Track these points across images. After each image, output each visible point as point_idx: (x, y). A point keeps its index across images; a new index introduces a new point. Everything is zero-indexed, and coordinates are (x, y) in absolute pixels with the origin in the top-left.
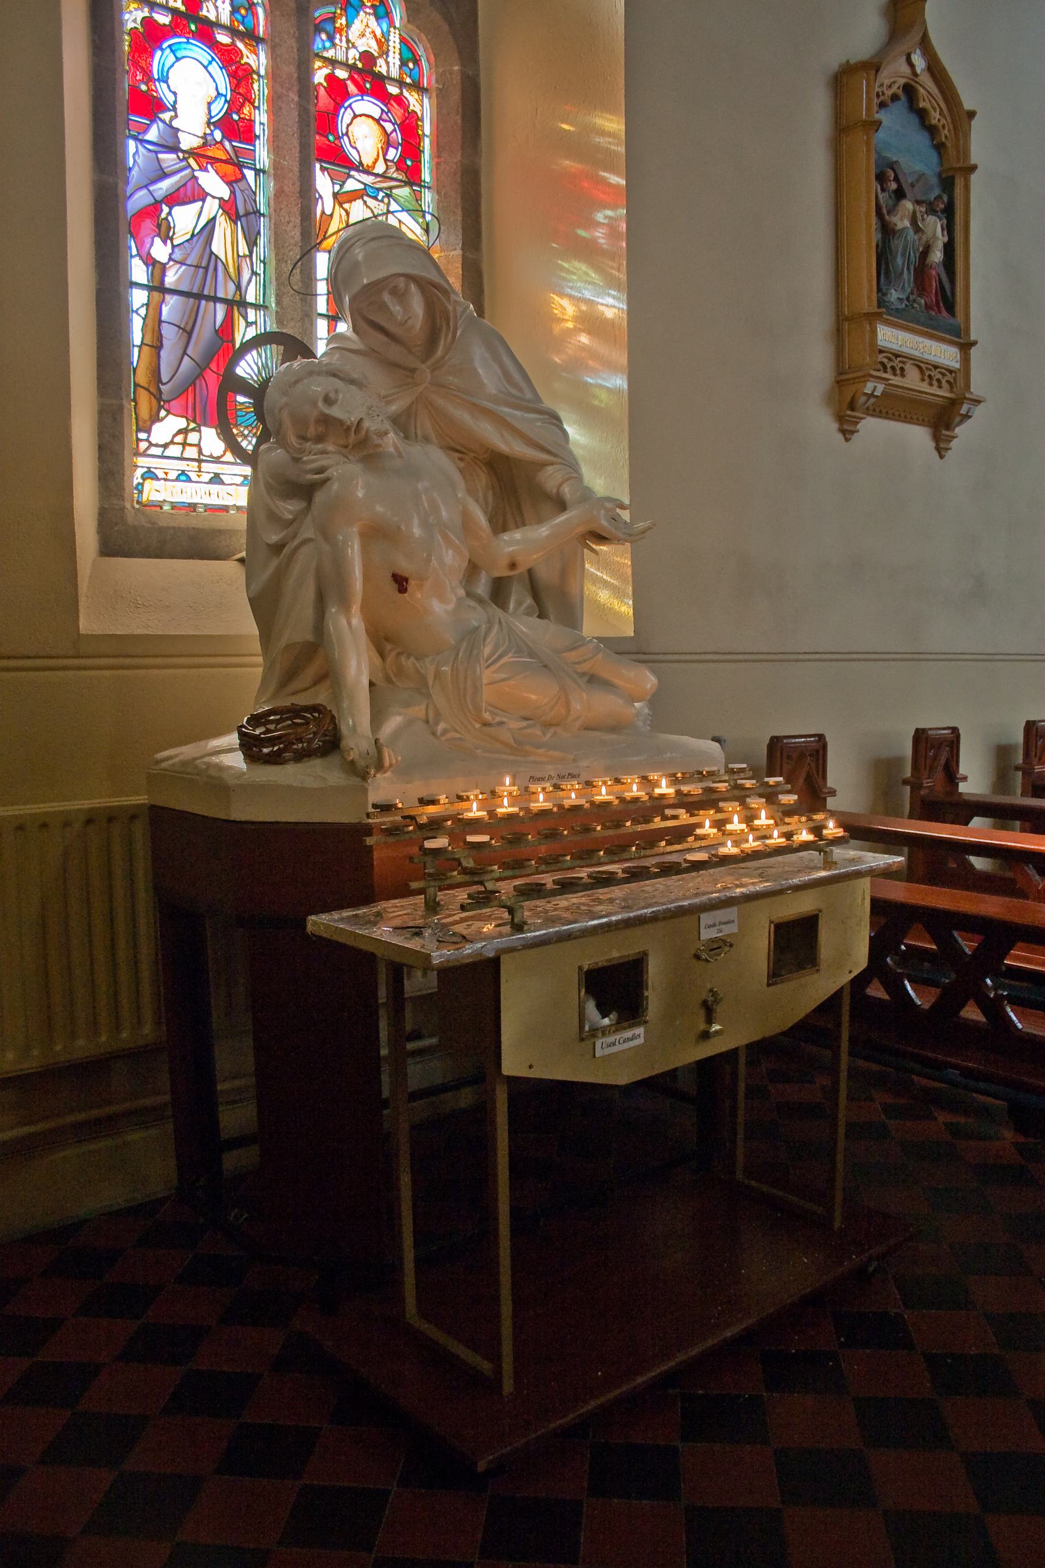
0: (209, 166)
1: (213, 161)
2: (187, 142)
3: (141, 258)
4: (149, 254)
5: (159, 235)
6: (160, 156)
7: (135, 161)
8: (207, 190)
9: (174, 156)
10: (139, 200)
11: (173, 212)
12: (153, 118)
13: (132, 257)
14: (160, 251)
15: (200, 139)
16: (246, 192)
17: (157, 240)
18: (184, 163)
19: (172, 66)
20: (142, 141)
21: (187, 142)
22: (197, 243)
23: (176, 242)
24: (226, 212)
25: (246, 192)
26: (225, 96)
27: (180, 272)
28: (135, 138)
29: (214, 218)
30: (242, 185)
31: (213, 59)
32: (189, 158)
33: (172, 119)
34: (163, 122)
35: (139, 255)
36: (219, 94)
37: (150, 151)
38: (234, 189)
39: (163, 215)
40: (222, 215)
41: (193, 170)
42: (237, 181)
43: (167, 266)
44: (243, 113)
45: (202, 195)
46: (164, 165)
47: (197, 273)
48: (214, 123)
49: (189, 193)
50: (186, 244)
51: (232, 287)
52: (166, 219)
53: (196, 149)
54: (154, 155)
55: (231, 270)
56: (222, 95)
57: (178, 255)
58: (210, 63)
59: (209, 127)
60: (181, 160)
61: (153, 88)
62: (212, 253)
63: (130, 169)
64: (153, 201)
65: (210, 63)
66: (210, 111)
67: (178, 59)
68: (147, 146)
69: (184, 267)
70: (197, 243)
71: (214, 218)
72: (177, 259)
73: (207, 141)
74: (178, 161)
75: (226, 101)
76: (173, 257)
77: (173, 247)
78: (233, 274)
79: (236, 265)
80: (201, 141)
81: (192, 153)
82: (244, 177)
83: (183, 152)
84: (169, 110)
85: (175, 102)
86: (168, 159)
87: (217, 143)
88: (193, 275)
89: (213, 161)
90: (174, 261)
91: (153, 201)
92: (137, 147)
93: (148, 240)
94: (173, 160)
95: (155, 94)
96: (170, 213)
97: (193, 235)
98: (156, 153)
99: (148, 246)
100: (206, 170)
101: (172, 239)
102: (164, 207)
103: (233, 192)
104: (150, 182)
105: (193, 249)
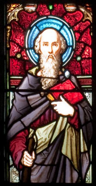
0: (61, 98)
1: (65, 92)
2: (46, 84)
3: (15, 167)
4: (20, 163)
5: (26, 149)
6: (29, 97)
7: (13, 105)
8: (59, 113)
9: (38, 95)
10: (16, 127)
11: (37, 133)
12: (25, 73)
13: (10, 166)
14: (28, 160)
15: (55, 80)
16: (86, 108)
17: (26, 153)
18: (45, 98)
19: (37, 37)
20: (18, 91)
21: (46, 84)
22: (51, 150)
23: (38, 152)
24: (72, 125)
25: (86, 108)
26: (72, 46)
27: (41, 171)
28: (14, 90)
29: (64, 130)
30: (84, 104)
31: (64, 24)
32: (47, 94)
33: (37, 71)
34: (32, 74)
35: (14, 164)
36: (67, 47)
37: (23, 96)
38: (78, 108)
39: (30, 136)
40: (69, 127)
41: (51, 101)
42: (80, 102)
43: (32, 169)
44: (84, 55)
45: (56, 116)
46: (31, 103)
47: (52, 169)
48: (64, 67)
49: (47, 118)
50: (45, 152)
51: (75, 175)
52: (32, 137)
53: (52, 87)
54: (25, 98)
55: (75, 163)
56: (70, 46)
57: (39, 160)
58: (62, 27)
59: (61, 70)
60: (42, 97)
61: (25, 54)
62: (61, 154)
63: (10, 110)
64: (23, 127)
65: (62, 27)
66: (61, 59)
67: (41, 32)
68: (20, 93)
69: (43, 167)
70: (51, 150)
71: (64, 130)
72: (38, 163)
73: (58, 80)
74: (40, 98)
75: (72, 50)
76: (36, 162)
77: (36, 155)
78: (76, 167)
79: (78, 159)
80: (56, 81)
81: (49, 91)
82: (85, 97)
83: (44, 91)
84: (35, 66)
85: (39, 59)
86: (34, 98)
87: (66, 79)
88: (49, 172)
89: (64, 92)
90: (36, 164)
91: (23, 127)
92: (14, 95)
93: (19, 154)
94: (37, 98)
95: (26, 58)
96: (34, 134)
97: (50, 145)
98: (26, 96)
99: (20, 157)
100: (59, 100)
101: (35, 150)
102: (31, 130)
103: (77, 111)
104: (21, 116)
105: (49, 154)
